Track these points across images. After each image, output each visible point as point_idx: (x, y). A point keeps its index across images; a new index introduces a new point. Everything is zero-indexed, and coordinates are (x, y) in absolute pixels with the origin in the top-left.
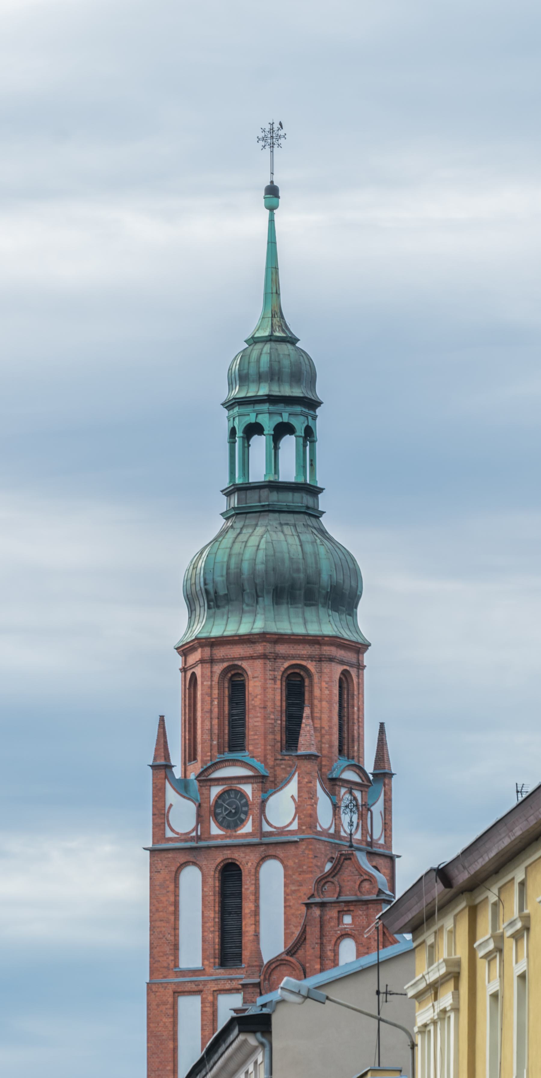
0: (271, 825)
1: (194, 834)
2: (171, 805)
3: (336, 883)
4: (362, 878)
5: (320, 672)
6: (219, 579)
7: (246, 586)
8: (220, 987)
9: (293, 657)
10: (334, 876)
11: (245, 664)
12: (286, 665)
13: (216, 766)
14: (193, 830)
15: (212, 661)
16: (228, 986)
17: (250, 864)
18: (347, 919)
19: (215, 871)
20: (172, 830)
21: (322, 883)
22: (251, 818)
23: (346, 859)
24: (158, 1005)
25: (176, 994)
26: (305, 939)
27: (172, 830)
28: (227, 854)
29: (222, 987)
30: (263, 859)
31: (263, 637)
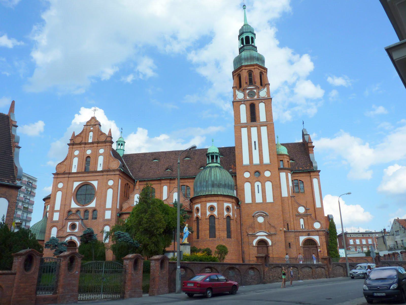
0: (261, 96)
1: (243, 99)
2: (237, 94)
11: (252, 70)
15: (245, 69)
20: (238, 98)
27: (238, 98)
30: (260, 102)
31: (257, 65)
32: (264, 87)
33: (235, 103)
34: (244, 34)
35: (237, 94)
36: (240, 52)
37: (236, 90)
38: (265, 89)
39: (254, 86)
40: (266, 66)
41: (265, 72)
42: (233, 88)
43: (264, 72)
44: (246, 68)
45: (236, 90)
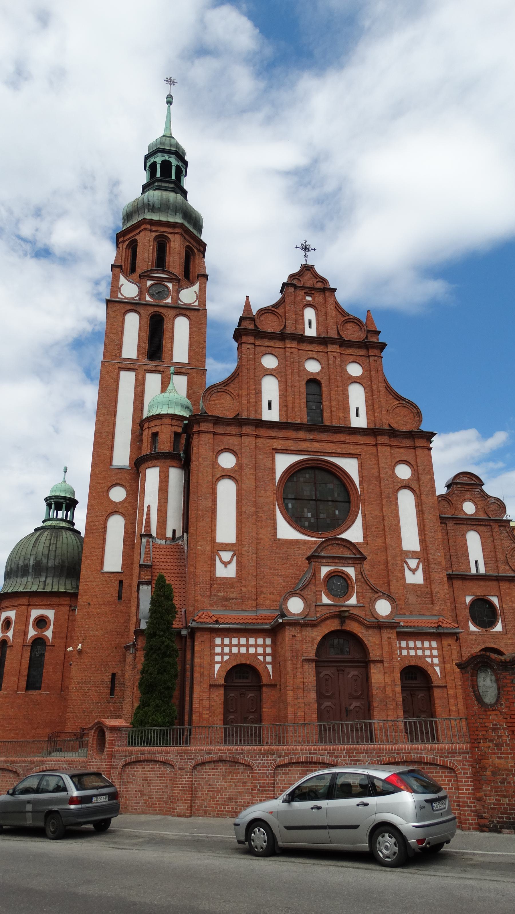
0: (182, 302)
2: (123, 285)
3: (301, 279)
4: (317, 280)
5: (199, 255)
6: (156, 201)
7: (171, 206)
8: (149, 368)
9: (190, 243)
10: (299, 277)
11: (169, 236)
12: (188, 244)
13: (152, 271)
14: (136, 297)
15: (151, 230)
16: (153, 369)
17: (170, 316)
18: (309, 298)
19: (148, 316)
20: (122, 295)
21: (292, 278)
22: (171, 297)
23: (306, 270)
24: (108, 372)
25: (120, 369)
26: (284, 301)
27: (122, 295)
28: (157, 309)
29: (150, 369)
30: (178, 315)
31: (181, 225)
32: (191, 283)
33: (113, 306)
34: (160, 154)
35: (120, 284)
36: (143, 192)
37: (121, 276)
38: (196, 287)
39: (168, 272)
40: (204, 238)
41: (199, 251)
42: (112, 266)
43: (197, 248)
44: (154, 228)
45: (121, 276)
